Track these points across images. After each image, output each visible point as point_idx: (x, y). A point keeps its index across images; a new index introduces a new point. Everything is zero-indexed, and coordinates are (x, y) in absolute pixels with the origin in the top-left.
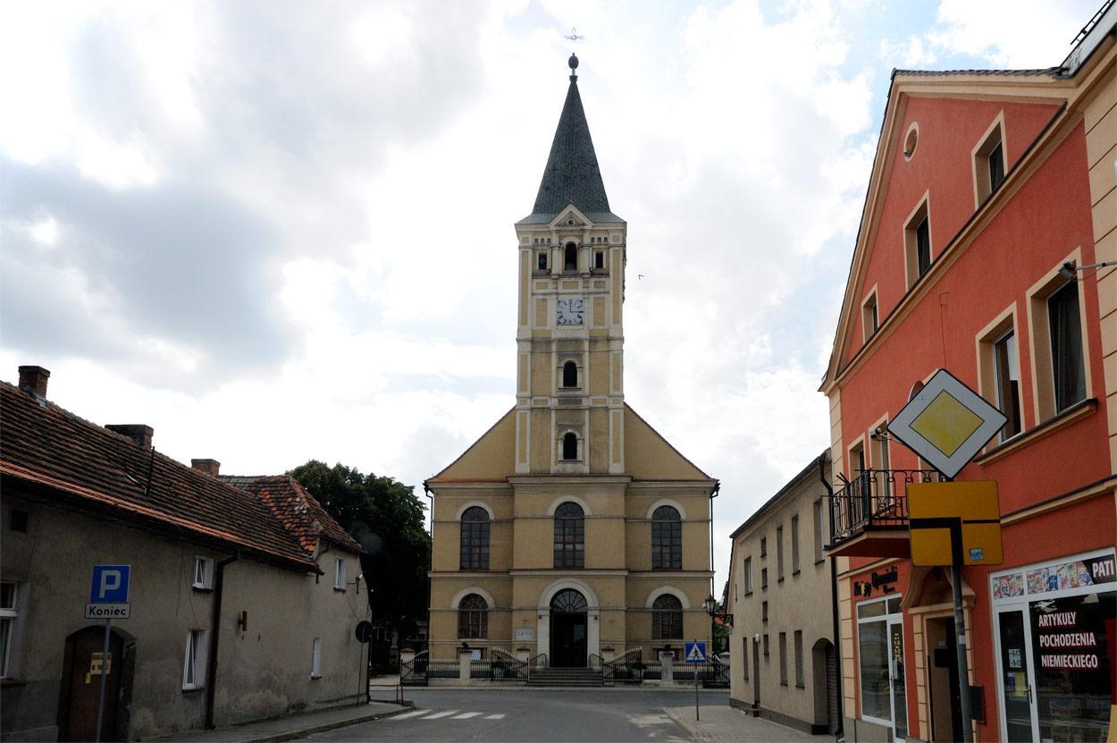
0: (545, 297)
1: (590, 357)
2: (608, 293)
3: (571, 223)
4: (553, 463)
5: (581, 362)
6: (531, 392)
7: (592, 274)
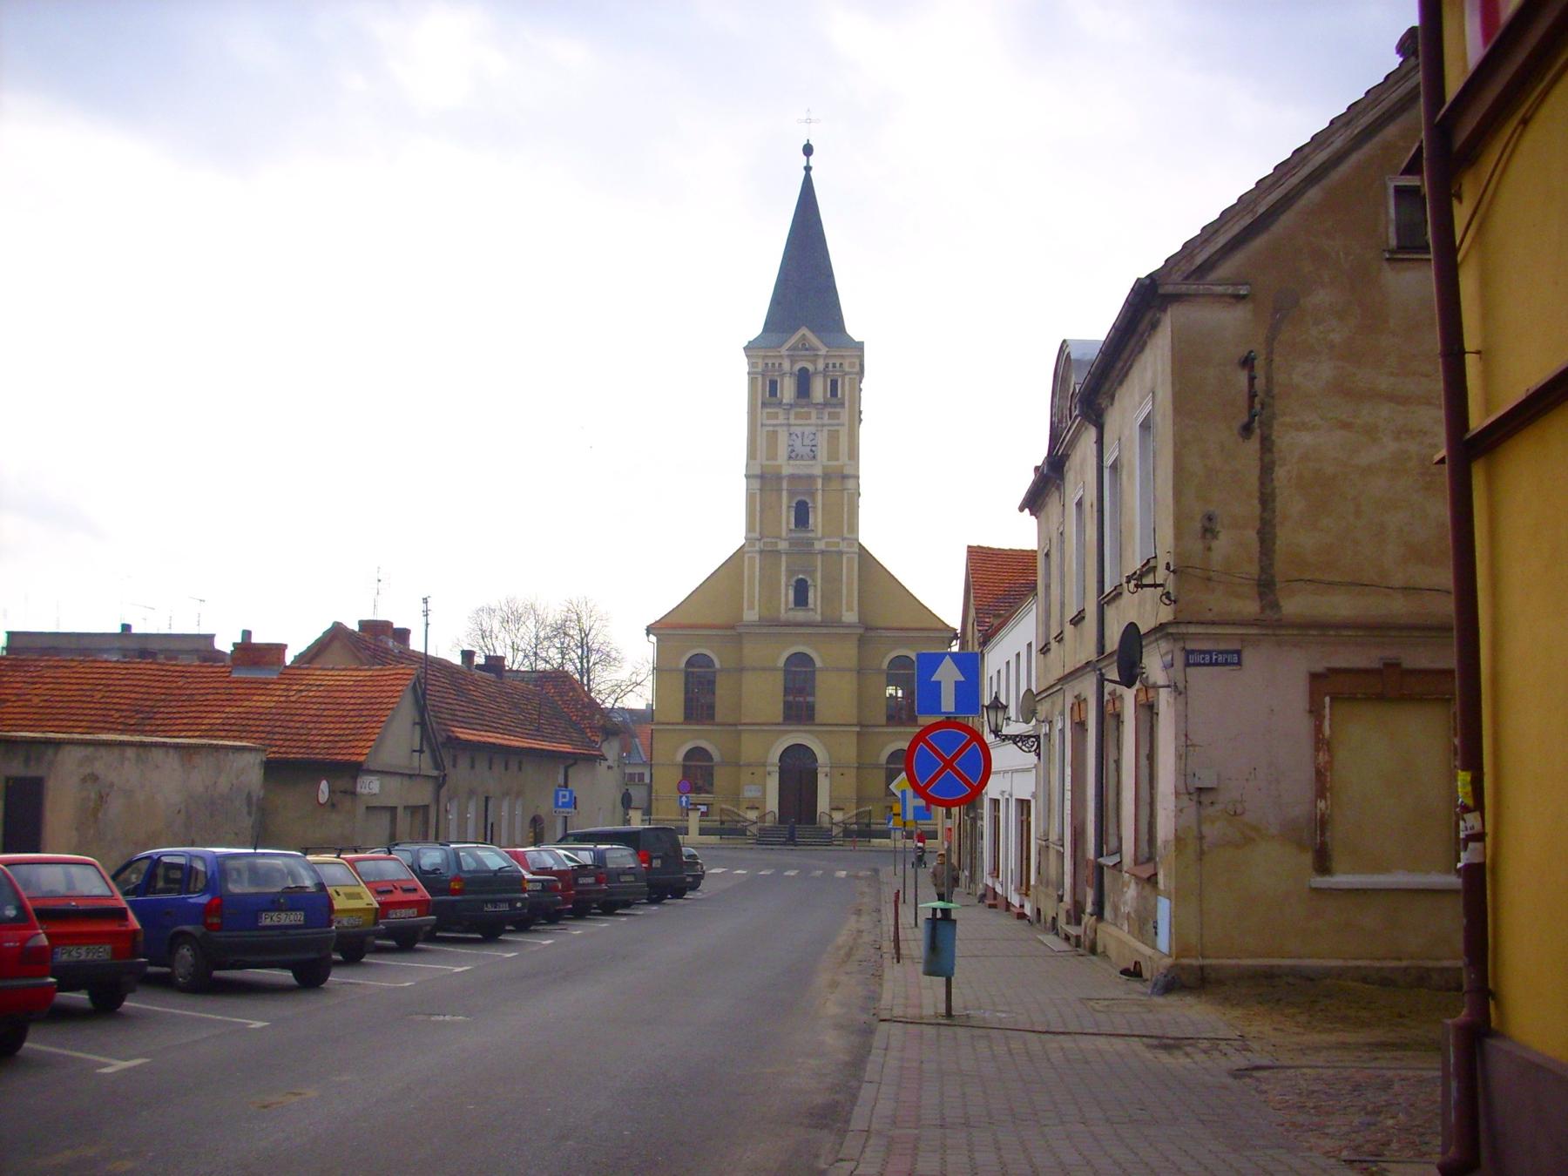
0: (776, 429)
1: (823, 496)
2: (843, 425)
4: (783, 611)
5: (814, 501)
7: (825, 405)
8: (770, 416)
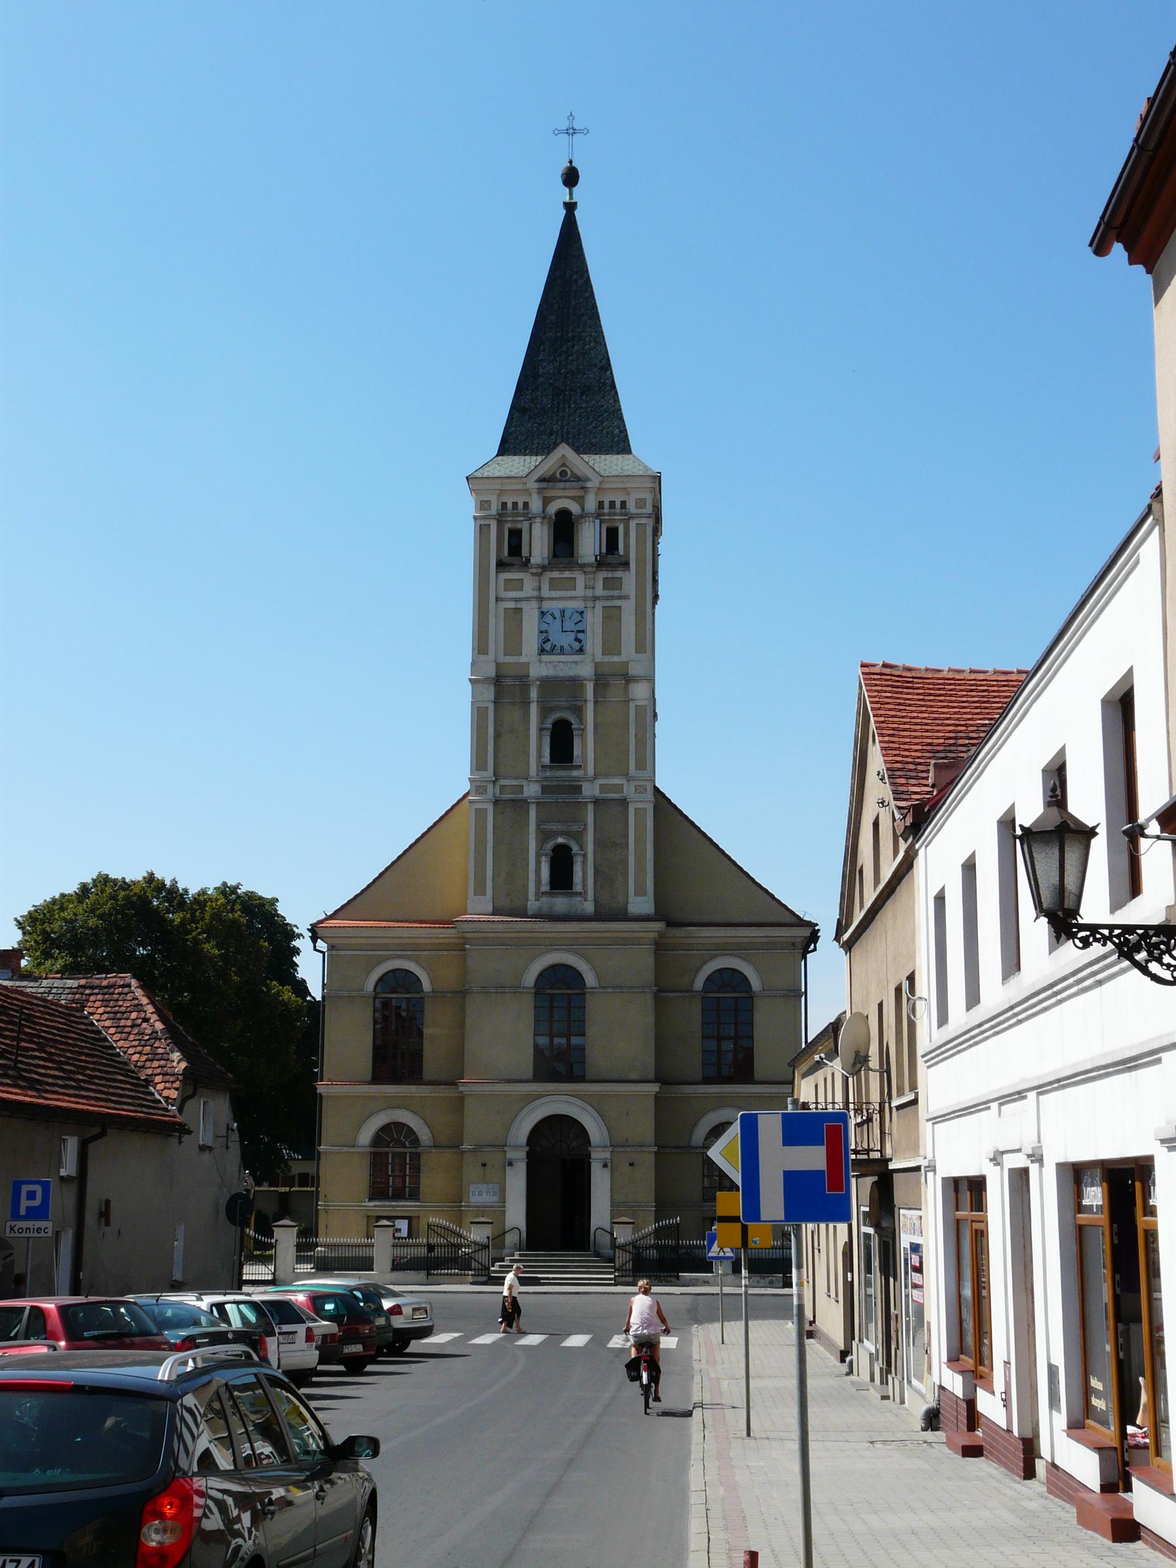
0: (519, 605)
2: (626, 597)
3: (563, 473)
4: (531, 896)
5: (581, 720)
6: (495, 774)
8: (510, 585)
